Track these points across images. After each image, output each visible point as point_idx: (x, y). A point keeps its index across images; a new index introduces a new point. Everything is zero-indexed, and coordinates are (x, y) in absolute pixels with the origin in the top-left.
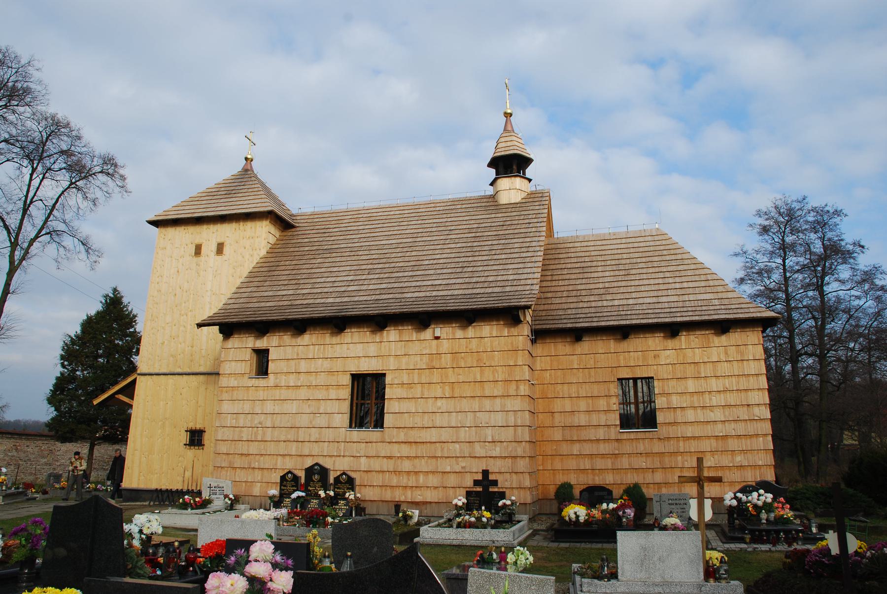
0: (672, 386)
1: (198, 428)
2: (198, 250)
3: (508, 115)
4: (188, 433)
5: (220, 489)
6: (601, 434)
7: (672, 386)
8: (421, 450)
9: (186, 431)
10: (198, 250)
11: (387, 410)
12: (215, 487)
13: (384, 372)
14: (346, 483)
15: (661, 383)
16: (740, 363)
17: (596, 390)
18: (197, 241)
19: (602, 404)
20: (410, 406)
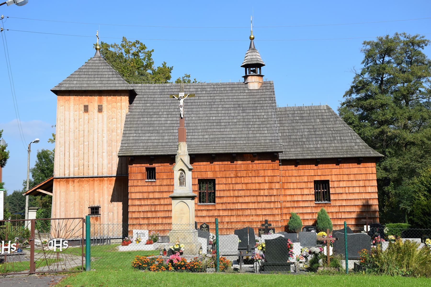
0: (336, 184)
1: (96, 206)
2: (86, 108)
3: (253, 39)
4: (90, 209)
5: (143, 234)
6: (306, 204)
7: (336, 184)
8: (234, 213)
9: (89, 208)
10: (86, 108)
11: (217, 195)
12: (140, 233)
13: (214, 178)
14: (205, 228)
15: (332, 183)
16: (366, 175)
17: (303, 185)
18: (87, 104)
19: (306, 192)
20: (227, 194)
